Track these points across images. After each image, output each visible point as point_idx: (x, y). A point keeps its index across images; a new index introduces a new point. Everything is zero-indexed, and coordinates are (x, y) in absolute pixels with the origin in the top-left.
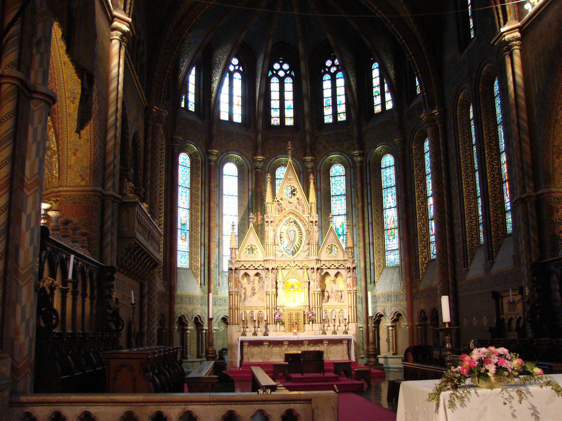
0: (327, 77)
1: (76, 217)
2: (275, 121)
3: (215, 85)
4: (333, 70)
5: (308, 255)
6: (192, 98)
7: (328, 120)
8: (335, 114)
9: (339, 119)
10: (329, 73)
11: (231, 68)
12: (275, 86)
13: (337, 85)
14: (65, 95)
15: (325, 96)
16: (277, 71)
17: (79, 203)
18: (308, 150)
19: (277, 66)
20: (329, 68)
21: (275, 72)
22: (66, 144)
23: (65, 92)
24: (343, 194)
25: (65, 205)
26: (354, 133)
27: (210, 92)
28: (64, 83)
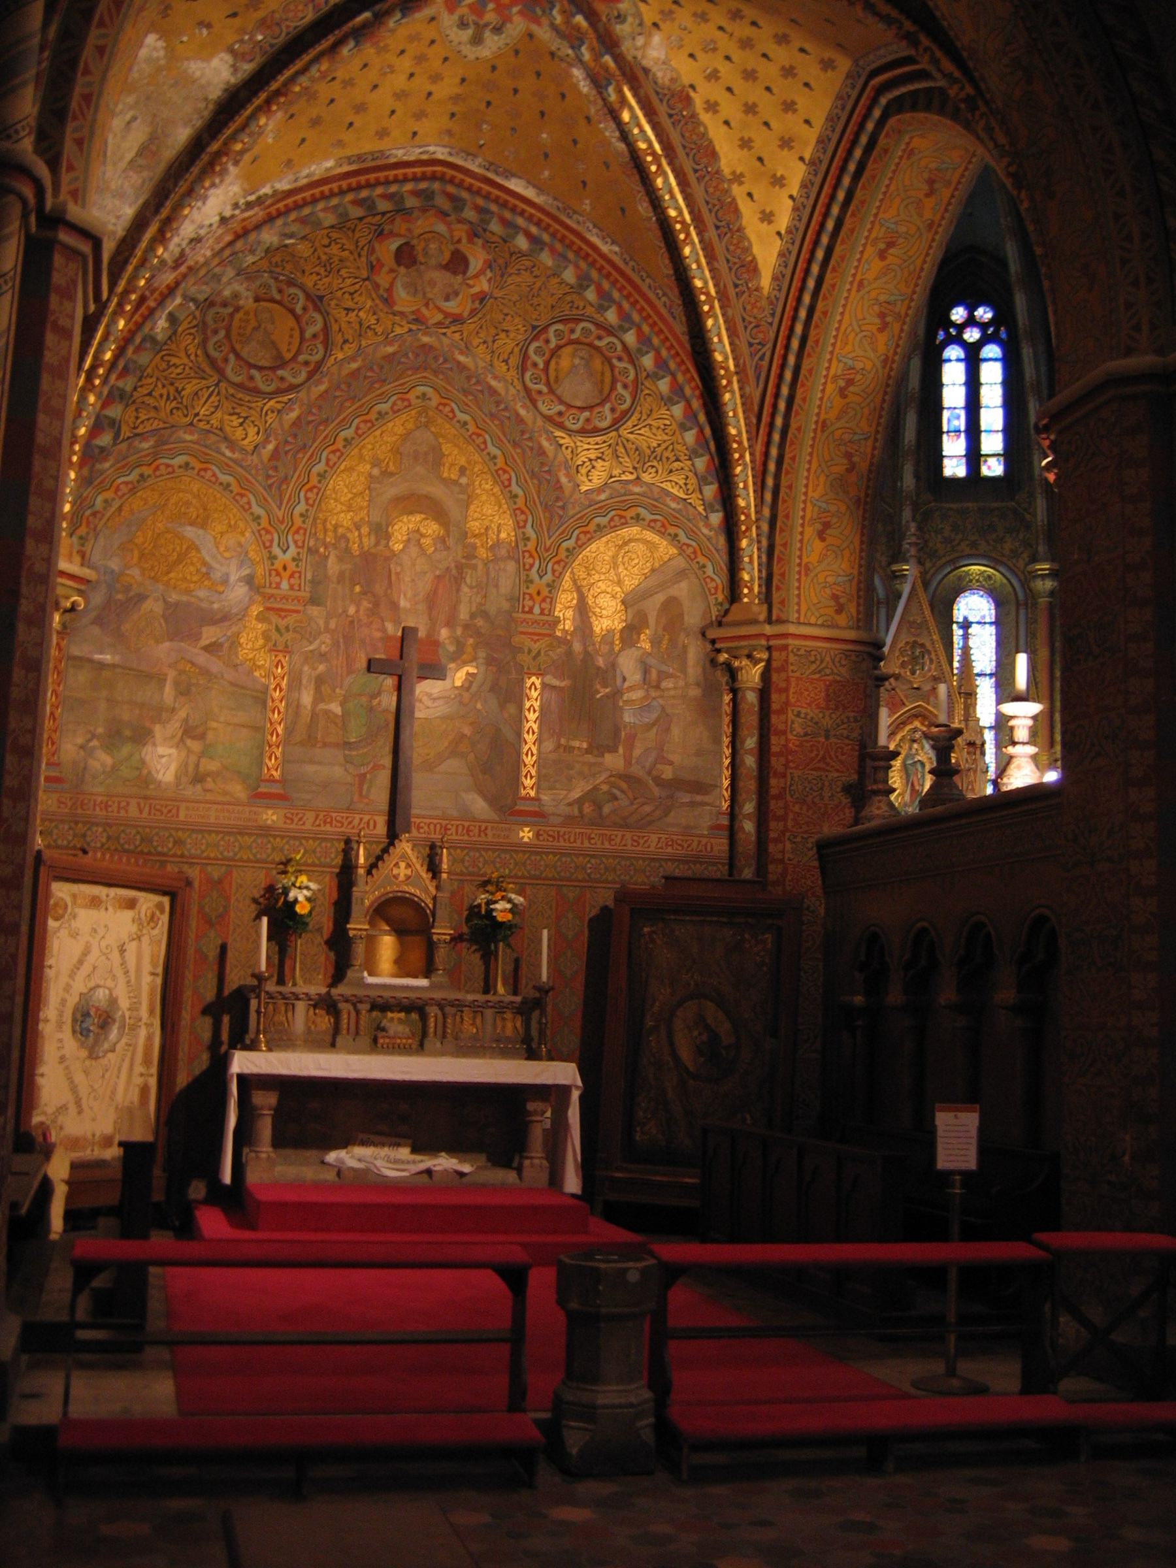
0: (954, 352)
1: (827, 713)
4: (971, 335)
7: (955, 468)
8: (974, 456)
9: (985, 471)
10: (959, 341)
13: (983, 379)
14: (828, 369)
15: (947, 402)
17: (832, 673)
20: (961, 328)
22: (802, 506)
23: (830, 361)
24: (988, 672)
25: (798, 674)
26: (1035, 516)
28: (836, 337)
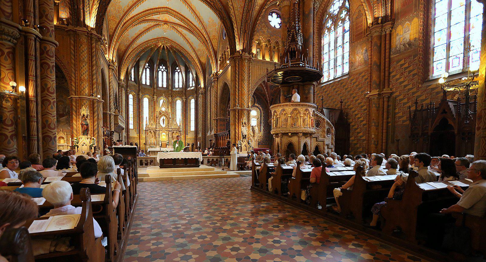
0: (177, 73)
2: (160, 85)
3: (140, 73)
4: (179, 71)
5: (168, 127)
6: (133, 76)
10: (177, 71)
11: (146, 67)
12: (160, 73)
16: (161, 69)
18: (170, 96)
19: (161, 67)
21: (160, 69)
27: (139, 75)
